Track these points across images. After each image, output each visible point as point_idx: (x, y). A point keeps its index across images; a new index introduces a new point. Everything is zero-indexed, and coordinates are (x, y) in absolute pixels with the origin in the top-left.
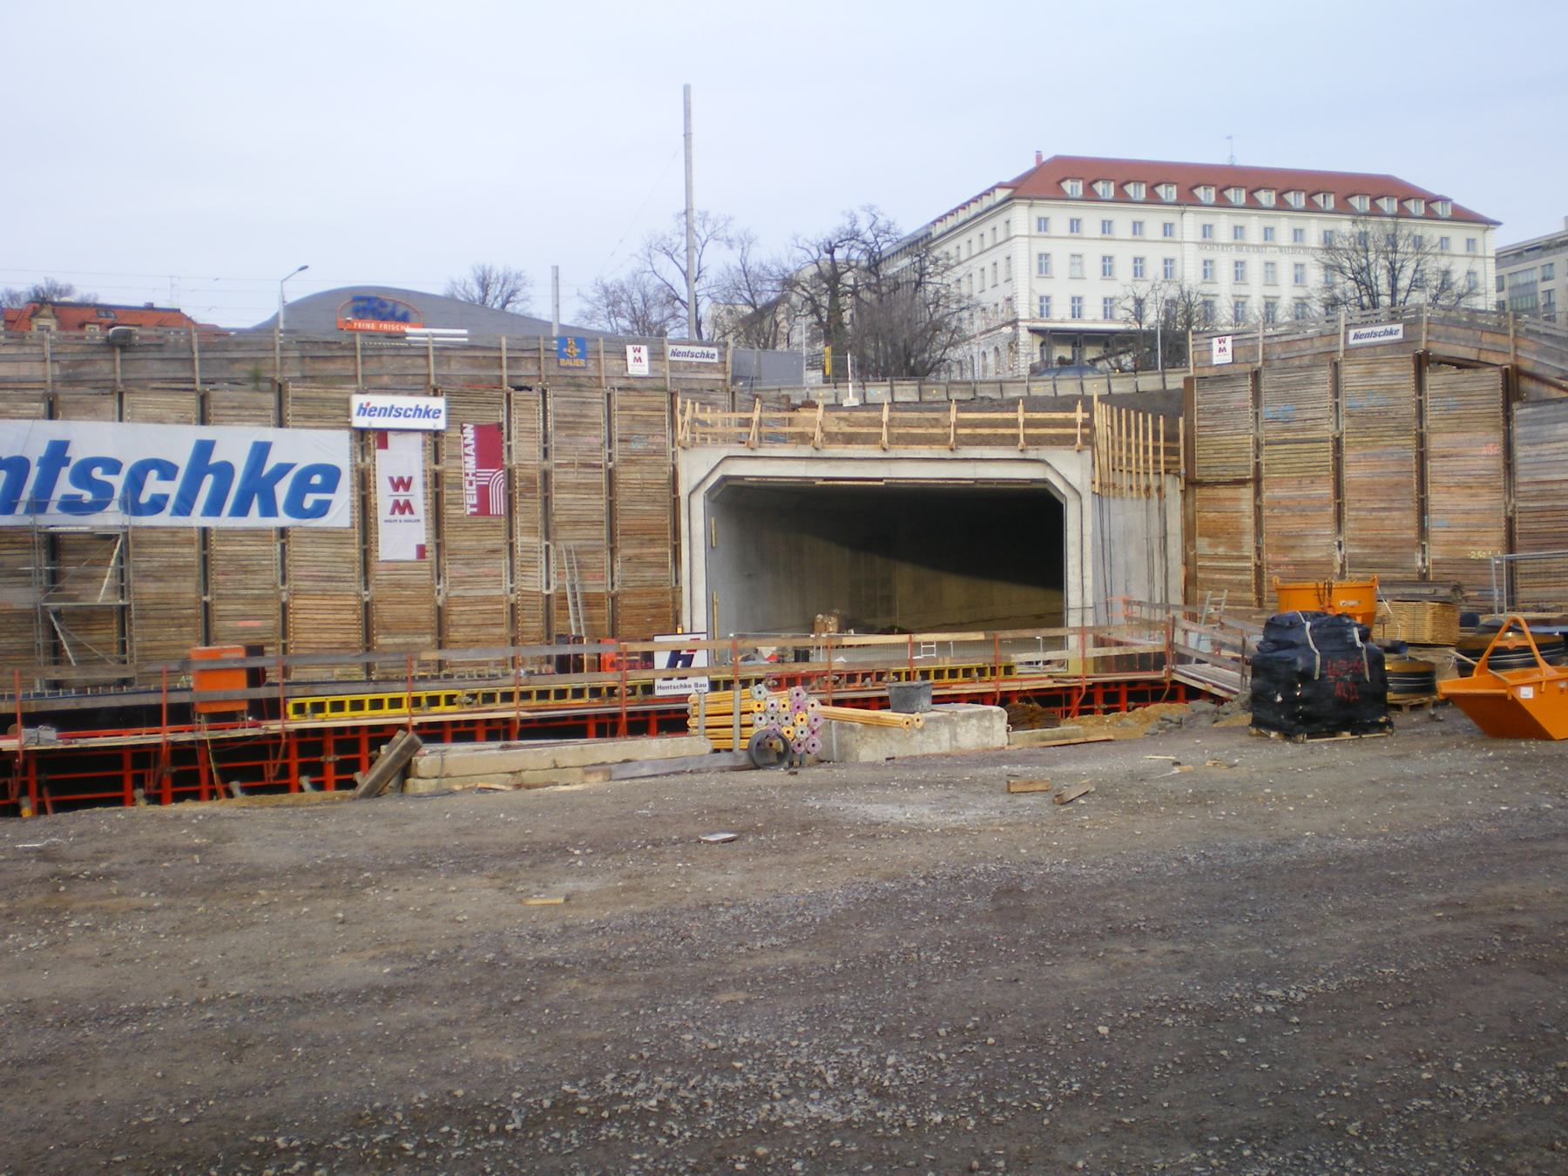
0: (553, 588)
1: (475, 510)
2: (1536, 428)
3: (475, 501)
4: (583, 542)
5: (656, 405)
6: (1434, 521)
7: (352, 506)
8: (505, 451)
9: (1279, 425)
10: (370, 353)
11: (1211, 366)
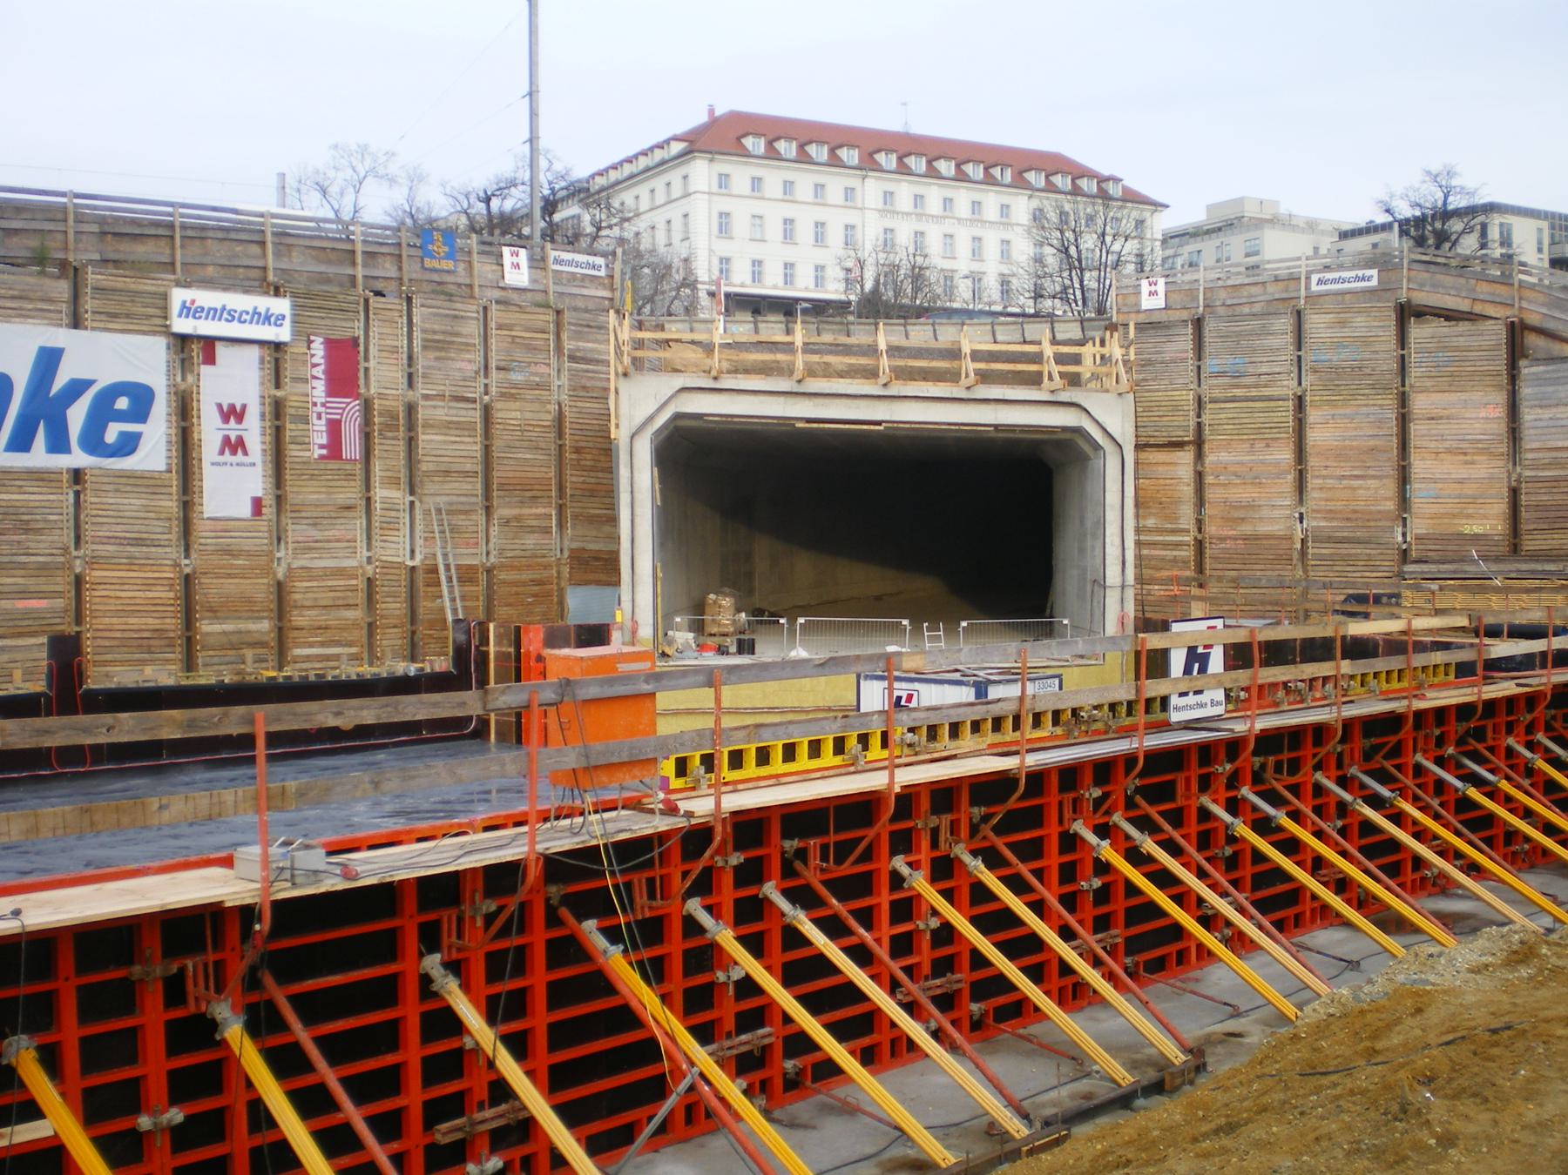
0: (419, 557)
1: (324, 452)
2: (1550, 389)
3: (324, 441)
4: (455, 499)
5: (540, 325)
6: (1417, 490)
7: (169, 442)
8: (361, 374)
9: (1226, 380)
10: (190, 233)
11: (1138, 312)
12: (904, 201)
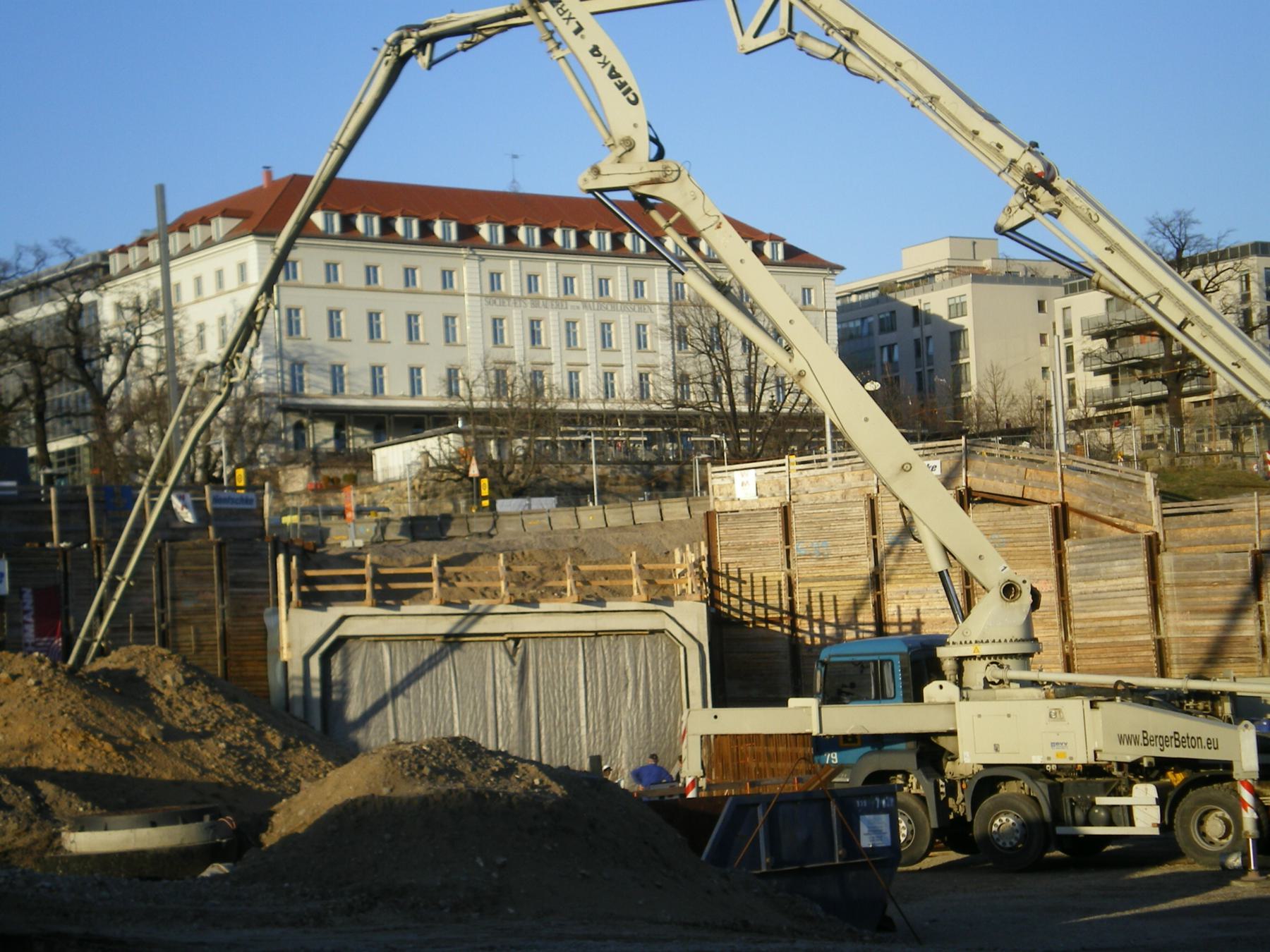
2: (1092, 565)
9: (812, 562)
12: (513, 282)
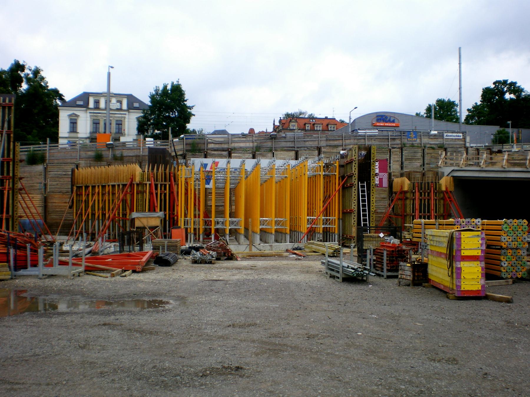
10: (347, 138)
